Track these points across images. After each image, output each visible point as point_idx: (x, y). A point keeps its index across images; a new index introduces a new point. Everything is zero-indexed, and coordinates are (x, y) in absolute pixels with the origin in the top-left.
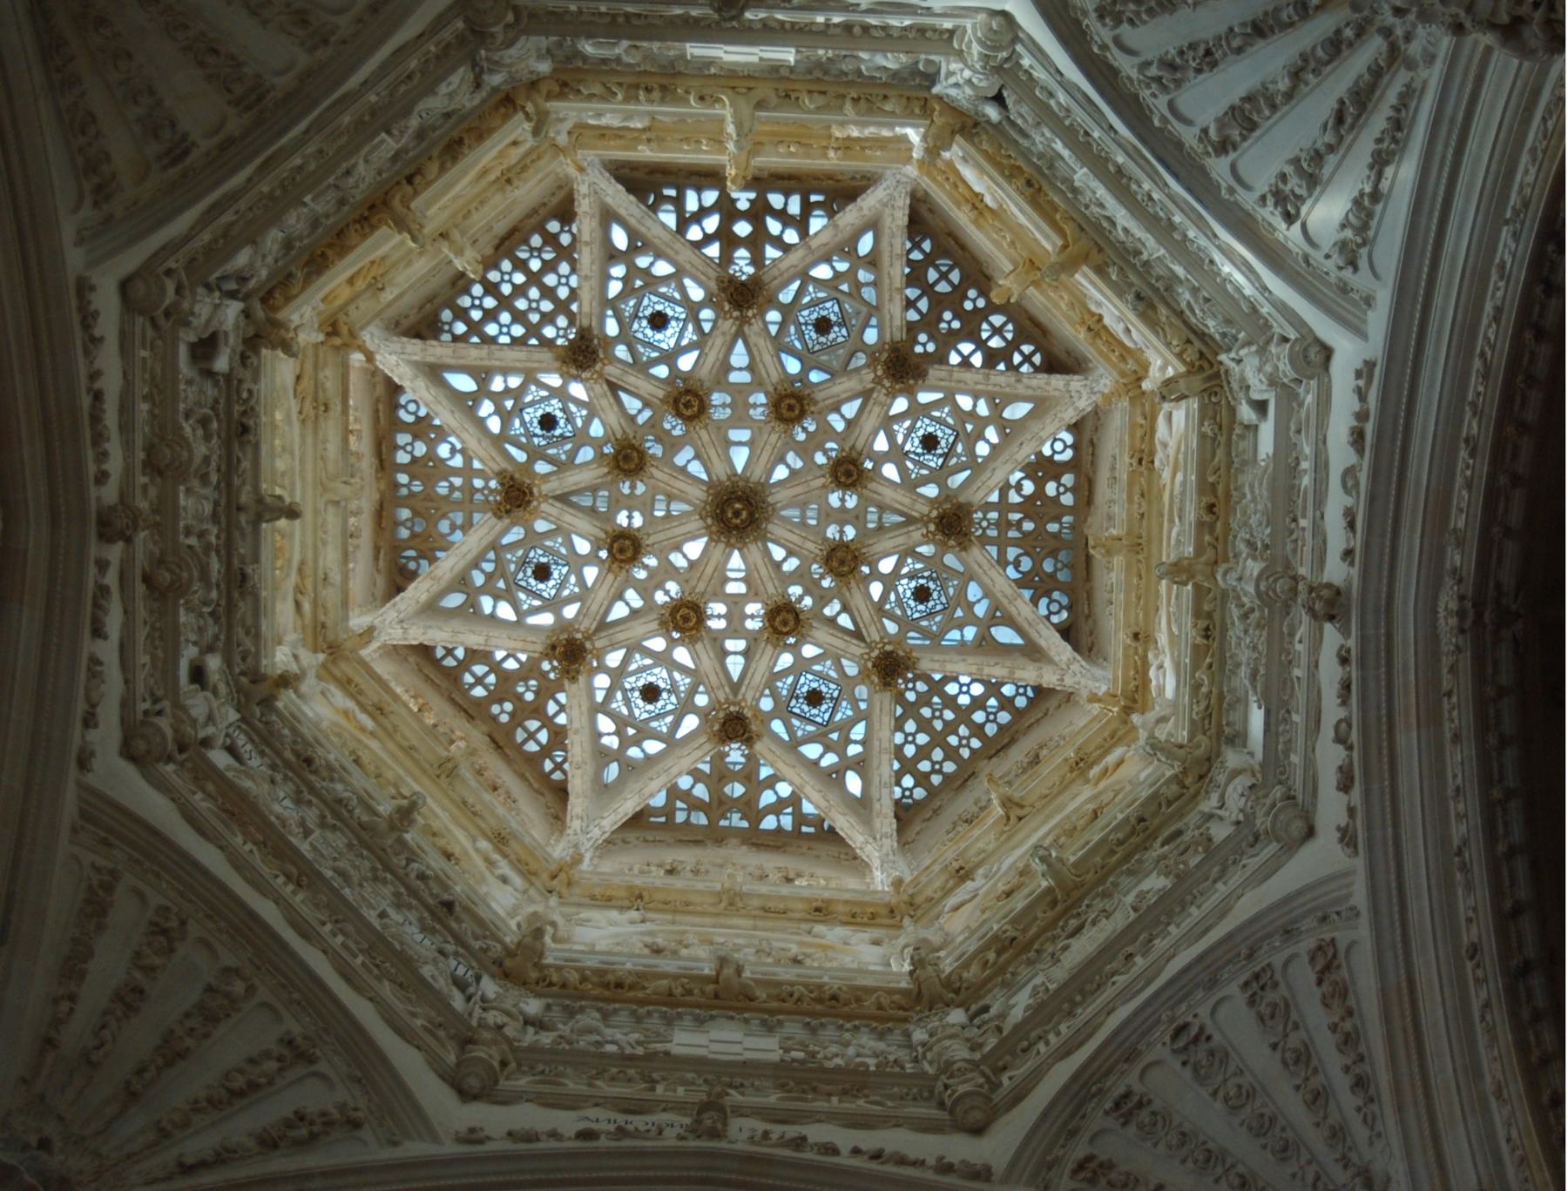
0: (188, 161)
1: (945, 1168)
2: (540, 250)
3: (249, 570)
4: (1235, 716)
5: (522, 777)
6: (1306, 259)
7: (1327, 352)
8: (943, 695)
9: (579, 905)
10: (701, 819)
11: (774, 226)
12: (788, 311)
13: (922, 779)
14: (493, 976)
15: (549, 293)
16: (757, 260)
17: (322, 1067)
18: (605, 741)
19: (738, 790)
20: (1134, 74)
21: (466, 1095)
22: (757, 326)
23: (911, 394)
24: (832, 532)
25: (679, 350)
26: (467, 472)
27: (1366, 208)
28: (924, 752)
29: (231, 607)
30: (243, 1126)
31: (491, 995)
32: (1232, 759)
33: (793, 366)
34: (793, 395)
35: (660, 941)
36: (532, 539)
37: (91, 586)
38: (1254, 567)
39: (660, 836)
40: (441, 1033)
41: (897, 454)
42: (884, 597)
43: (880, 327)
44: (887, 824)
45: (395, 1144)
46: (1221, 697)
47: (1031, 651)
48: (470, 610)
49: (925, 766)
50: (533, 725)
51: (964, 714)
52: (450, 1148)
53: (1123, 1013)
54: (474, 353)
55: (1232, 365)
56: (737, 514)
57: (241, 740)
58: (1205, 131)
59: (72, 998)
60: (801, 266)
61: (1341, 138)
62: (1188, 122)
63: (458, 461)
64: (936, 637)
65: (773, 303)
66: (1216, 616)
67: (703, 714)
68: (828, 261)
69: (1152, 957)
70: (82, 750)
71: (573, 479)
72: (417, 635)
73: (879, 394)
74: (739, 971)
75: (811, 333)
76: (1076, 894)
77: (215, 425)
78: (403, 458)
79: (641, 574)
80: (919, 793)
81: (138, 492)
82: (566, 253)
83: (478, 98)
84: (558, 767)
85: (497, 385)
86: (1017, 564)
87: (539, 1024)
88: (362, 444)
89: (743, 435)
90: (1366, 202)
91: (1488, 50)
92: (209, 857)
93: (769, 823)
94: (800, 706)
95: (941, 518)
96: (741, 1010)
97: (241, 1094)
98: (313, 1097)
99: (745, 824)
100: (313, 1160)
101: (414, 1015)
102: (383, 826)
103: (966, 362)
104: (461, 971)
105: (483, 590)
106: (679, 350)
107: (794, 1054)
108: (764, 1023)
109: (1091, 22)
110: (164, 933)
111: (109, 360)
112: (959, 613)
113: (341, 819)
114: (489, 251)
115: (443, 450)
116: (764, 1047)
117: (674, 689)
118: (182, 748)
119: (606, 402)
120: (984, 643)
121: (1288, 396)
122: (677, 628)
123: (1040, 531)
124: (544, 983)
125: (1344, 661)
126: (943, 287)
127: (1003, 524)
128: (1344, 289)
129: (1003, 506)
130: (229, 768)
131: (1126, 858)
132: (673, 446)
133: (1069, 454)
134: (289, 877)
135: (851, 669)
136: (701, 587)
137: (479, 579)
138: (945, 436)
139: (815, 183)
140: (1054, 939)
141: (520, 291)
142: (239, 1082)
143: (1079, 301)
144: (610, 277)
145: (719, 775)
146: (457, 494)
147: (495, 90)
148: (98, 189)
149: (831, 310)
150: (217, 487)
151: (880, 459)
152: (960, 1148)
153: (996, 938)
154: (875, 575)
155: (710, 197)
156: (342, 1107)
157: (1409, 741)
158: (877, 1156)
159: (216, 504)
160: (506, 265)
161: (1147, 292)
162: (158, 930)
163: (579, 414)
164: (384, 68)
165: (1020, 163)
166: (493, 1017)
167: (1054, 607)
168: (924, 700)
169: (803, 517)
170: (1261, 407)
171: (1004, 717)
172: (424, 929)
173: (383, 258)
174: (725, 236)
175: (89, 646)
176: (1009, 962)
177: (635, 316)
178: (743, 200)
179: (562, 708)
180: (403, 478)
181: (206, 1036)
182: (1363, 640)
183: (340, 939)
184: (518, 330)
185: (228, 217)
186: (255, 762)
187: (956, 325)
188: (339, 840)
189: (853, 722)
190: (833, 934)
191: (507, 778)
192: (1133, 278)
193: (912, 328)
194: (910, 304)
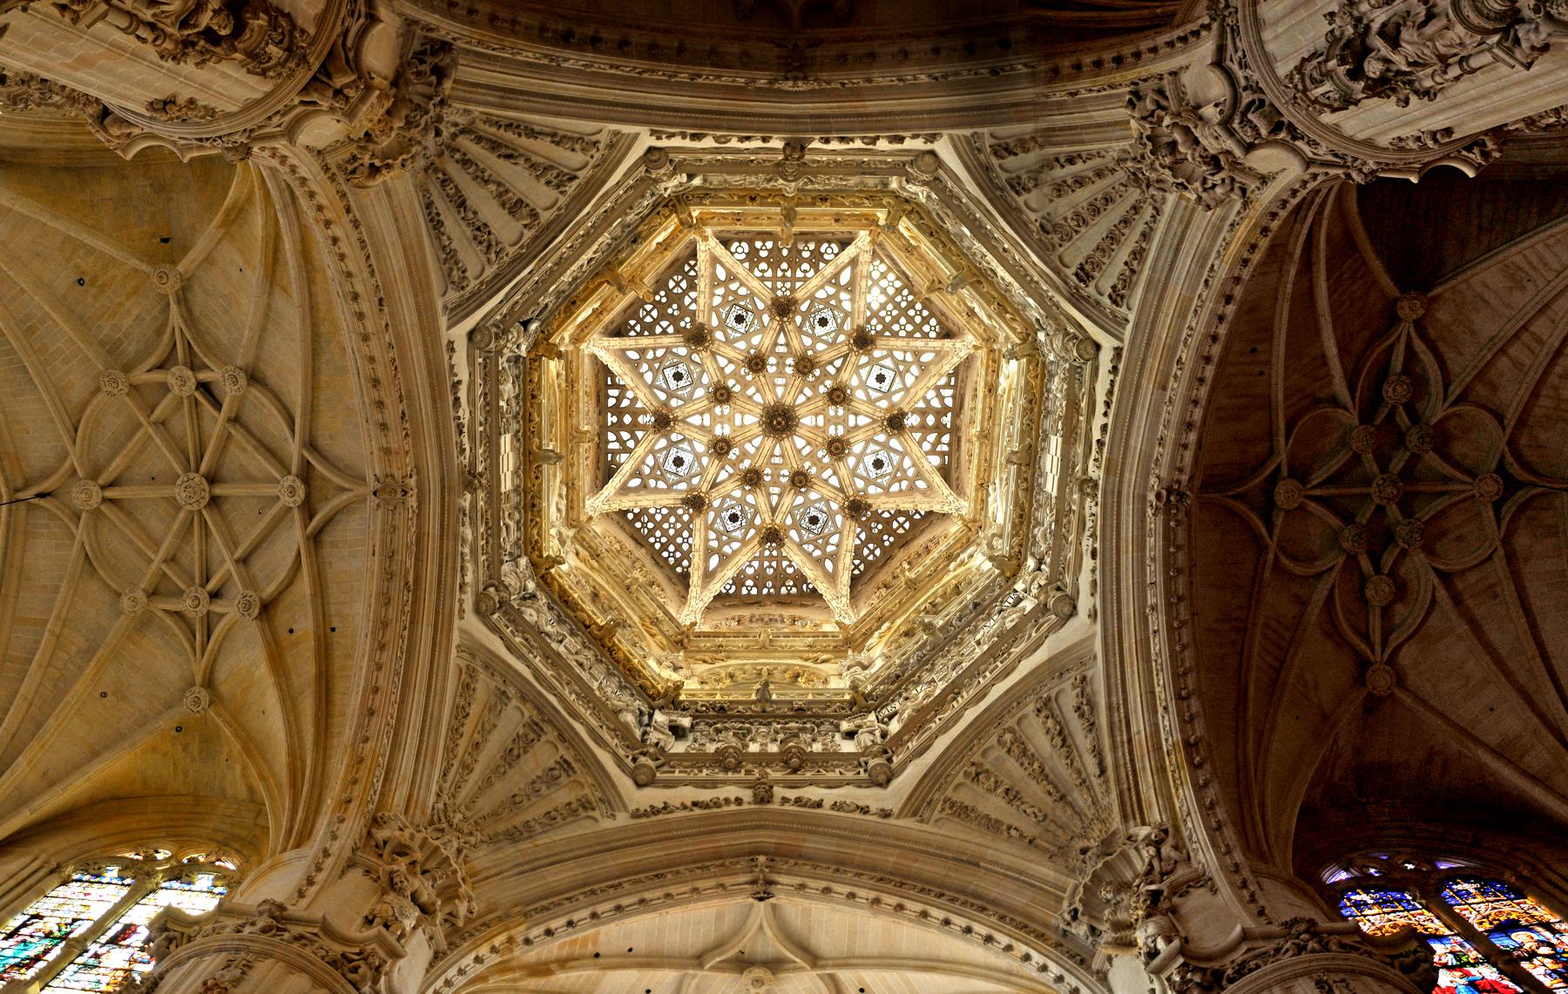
0: (570, 759)
5: (923, 531)
9: (986, 516)
10: (946, 438)
13: (925, 320)
14: (1015, 583)
15: (665, 518)
17: (1053, 693)
18: (904, 487)
20: (496, 267)
21: (1074, 611)
23: (711, 332)
25: (693, 451)
26: (761, 559)
28: (911, 320)
30: (1083, 741)
31: (1023, 586)
34: (715, 393)
36: (796, 526)
37: (794, 808)
40: (1041, 621)
44: (948, 343)
45: (1095, 657)
49: (918, 319)
50: (895, 525)
51: (891, 299)
52: (1098, 627)
54: (697, 559)
56: (779, 423)
57: (885, 712)
60: (647, 391)
61: (521, 155)
62: (522, 235)
64: (847, 314)
66: (814, 194)
67: (890, 436)
70: (880, 816)
71: (763, 506)
72: (846, 590)
77: (719, 725)
78: (754, 591)
80: (933, 322)
81: (749, 777)
82: (644, 511)
89: (738, 417)
90: (557, 139)
93: (949, 402)
94: (885, 386)
98: (1069, 699)
99: (949, 414)
101: (1030, 636)
104: (1010, 600)
105: (824, 551)
106: (693, 451)
107: (1060, 427)
112: (833, 302)
114: (643, 551)
115: (750, 571)
116: (1055, 442)
117: (877, 452)
118: (886, 752)
119: (722, 490)
122: (843, 452)
127: (784, 279)
129: (774, 279)
132: (744, 455)
134: (955, 699)
135: (864, 359)
136: (820, 440)
139: (601, 382)
141: (665, 533)
142: (1058, 740)
144: (656, 487)
145: (923, 428)
146: (774, 564)
148: (585, 808)
150: (751, 723)
154: (812, 347)
159: (761, 724)
160: (652, 540)
161: (631, 237)
163: (729, 502)
164: (520, 657)
165: (562, 308)
167: (829, 251)
168: (881, 320)
172: (989, 617)
173: (641, 618)
174: (634, 426)
175: (826, 810)
177: (676, 474)
180: (765, 591)
181: (1033, 755)
183: (987, 673)
184: (686, 534)
186: (897, 705)
187: (675, 306)
191: (922, 540)
192: (624, 244)
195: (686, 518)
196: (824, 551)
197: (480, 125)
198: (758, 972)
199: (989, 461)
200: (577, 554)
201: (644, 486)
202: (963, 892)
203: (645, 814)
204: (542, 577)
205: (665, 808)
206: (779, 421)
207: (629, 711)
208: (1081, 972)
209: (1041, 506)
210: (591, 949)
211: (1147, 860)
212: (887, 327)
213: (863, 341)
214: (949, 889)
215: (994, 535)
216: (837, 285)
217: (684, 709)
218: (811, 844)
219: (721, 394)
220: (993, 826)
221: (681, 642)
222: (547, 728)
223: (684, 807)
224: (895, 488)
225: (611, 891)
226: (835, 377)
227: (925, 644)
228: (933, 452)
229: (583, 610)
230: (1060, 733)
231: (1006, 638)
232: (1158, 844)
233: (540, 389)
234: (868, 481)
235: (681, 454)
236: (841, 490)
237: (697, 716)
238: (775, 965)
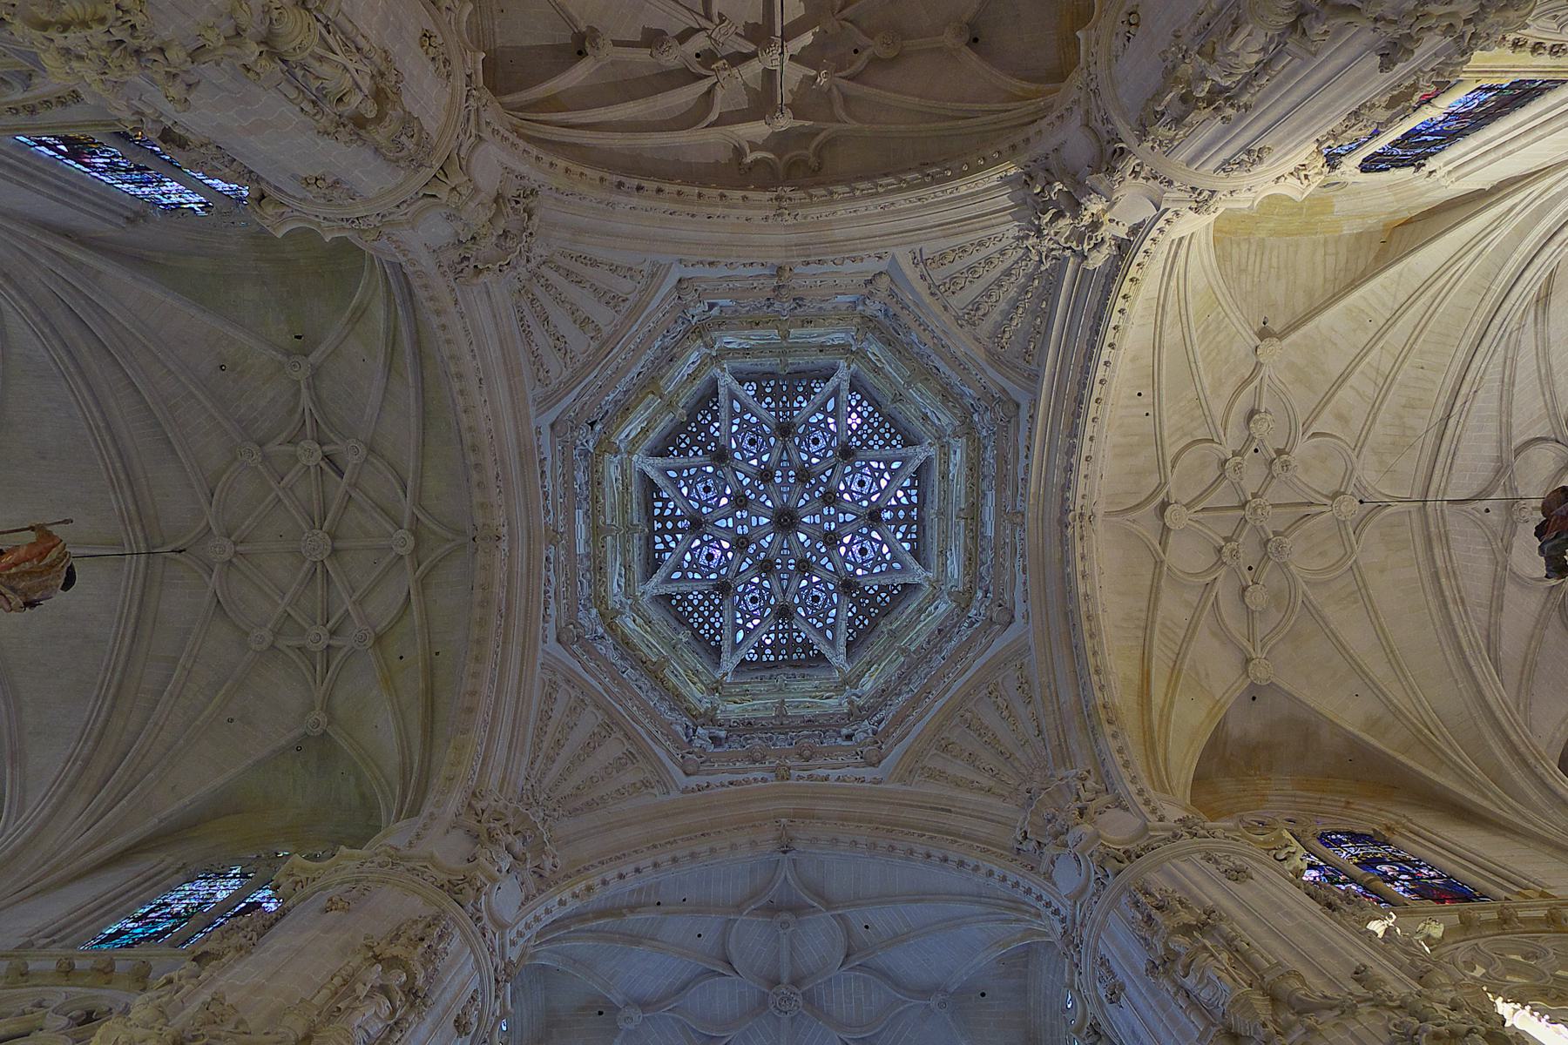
2: (684, 607)
3: (806, 719)
5: (900, 602)
8: (857, 429)
11: (668, 512)
12: (702, 504)
13: (893, 437)
15: (701, 602)
16: (681, 518)
17: (1000, 680)
19: (901, 514)
22: (708, 517)
24: (792, 480)
28: (882, 437)
33: (724, 501)
36: (802, 604)
39: (921, 544)
41: (758, 456)
42: (817, 457)
44: (910, 450)
47: (835, 393)
48: (832, 627)
49: (887, 436)
54: (727, 632)
55: (695, 319)
56: (786, 520)
58: (592, 338)
63: (772, 636)
68: (681, 488)
71: (776, 589)
72: (843, 649)
75: (710, 495)
79: (814, 558)
80: (899, 437)
82: (685, 595)
84: (896, 588)
85: (740, 621)
86: (800, 402)
89: (754, 519)
93: (914, 499)
95: (782, 436)
102: (908, 659)
104: (966, 625)
106: (721, 548)
108: (983, 498)
112: (822, 425)
113: (906, 677)
115: (768, 642)
116: (991, 495)
117: (862, 542)
119: (745, 578)
120: (834, 414)
124: (970, 592)
126: (688, 441)
131: (906, 350)
132: (760, 548)
137: (820, 625)
138: (749, 436)
139: (649, 496)
141: (701, 614)
143: (683, 384)
147: (605, 631)
149: (700, 486)
151: (760, 462)
155: (658, 539)
159: (780, 733)
162: (945, 749)
167: (818, 385)
168: (859, 438)
170: (711, 306)
172: (951, 639)
174: (673, 533)
175: (831, 782)
176: (953, 397)
178: (658, 525)
179: (871, 588)
180: (781, 657)
184: (717, 614)
185: (659, 737)
194: (696, 454)
198: (786, 916)
199: (945, 532)
200: (634, 621)
201: (684, 578)
203: (693, 791)
204: (608, 625)
205: (708, 786)
206: (785, 521)
209: (984, 549)
212: (864, 443)
213: (846, 453)
216: (824, 412)
219: (739, 501)
221: (717, 689)
224: (876, 570)
225: (668, 846)
228: (903, 540)
233: (603, 478)
234: (856, 566)
237: (730, 729)
238: (798, 909)
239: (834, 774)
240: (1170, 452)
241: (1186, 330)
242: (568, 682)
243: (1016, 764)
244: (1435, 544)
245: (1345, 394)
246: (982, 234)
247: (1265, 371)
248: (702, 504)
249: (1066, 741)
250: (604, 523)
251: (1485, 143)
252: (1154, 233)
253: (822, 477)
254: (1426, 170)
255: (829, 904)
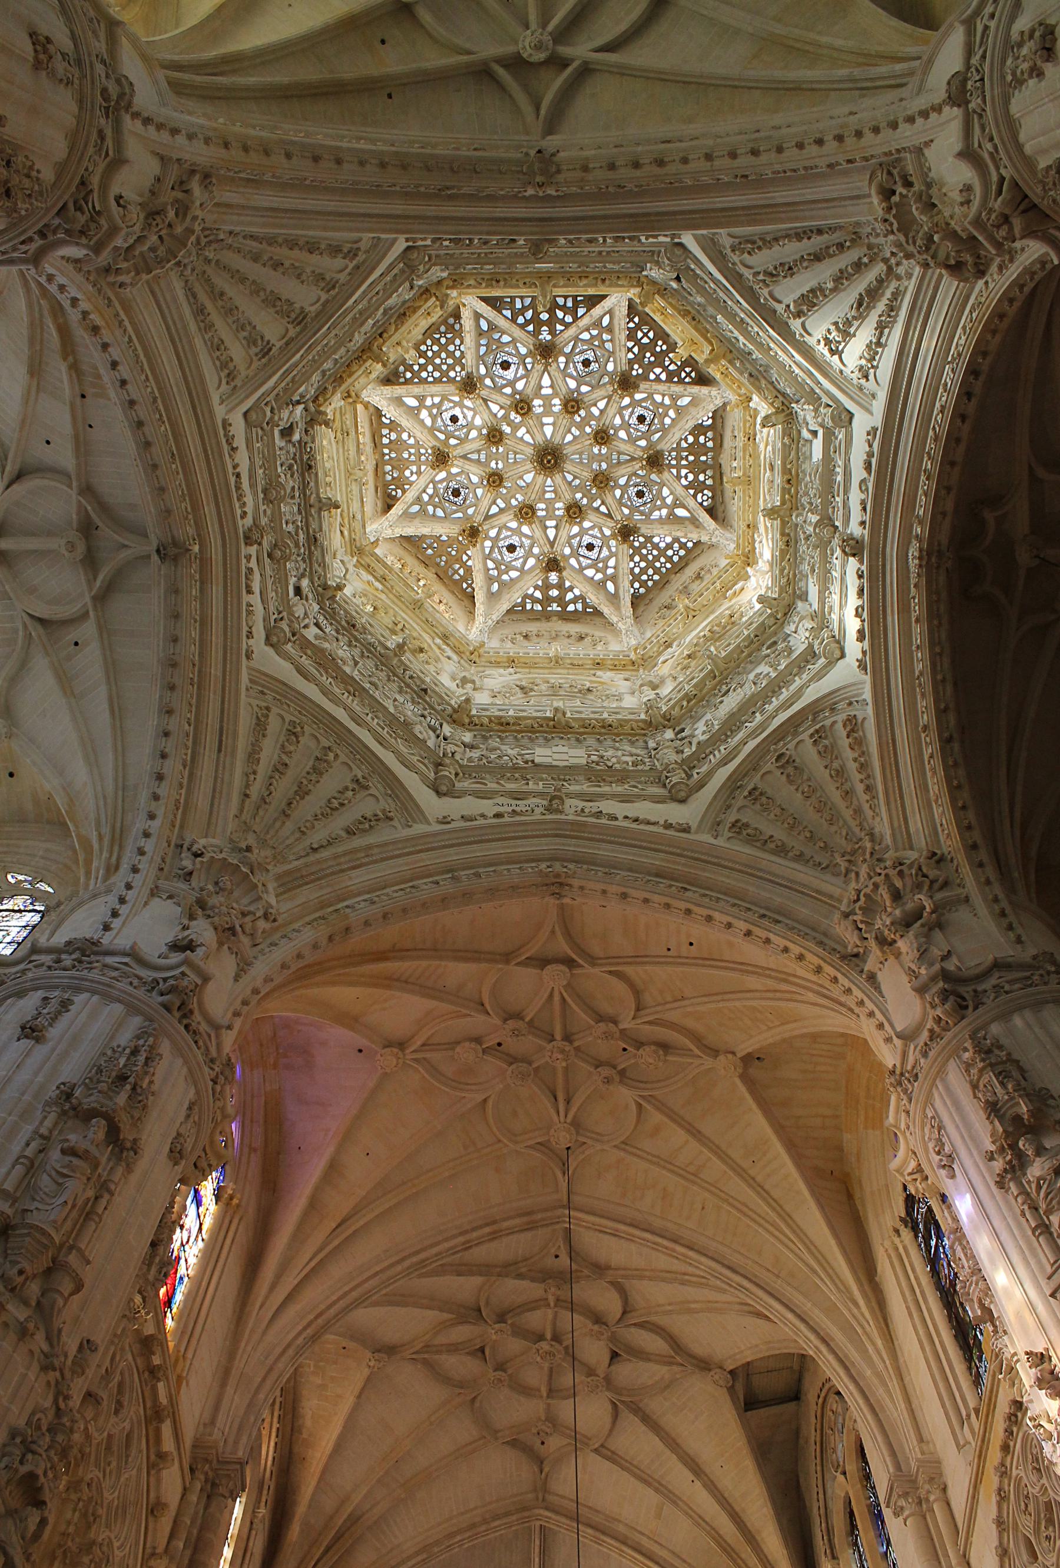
1: (668, 826)
4: (802, 584)
5: (453, 593)
6: (841, 372)
7: (851, 416)
11: (560, 314)
12: (569, 357)
13: (643, 584)
16: (552, 332)
17: (373, 791)
22: (554, 365)
24: (595, 466)
25: (517, 379)
27: (875, 347)
28: (643, 571)
29: (311, 553)
32: (800, 604)
33: (572, 384)
35: (524, 683)
38: (814, 518)
39: (519, 616)
41: (626, 425)
42: (622, 496)
43: (615, 362)
44: (627, 609)
46: (795, 575)
47: (694, 521)
51: (662, 552)
53: (752, 745)
54: (417, 390)
57: (321, 619)
58: (788, 306)
59: (255, 773)
65: (561, 353)
69: (766, 716)
72: (398, 532)
73: (616, 397)
74: (564, 714)
75: (580, 366)
76: (725, 673)
80: (642, 590)
83: (412, 293)
87: (472, 747)
88: (365, 439)
91: (941, 276)
92: (311, 691)
94: (583, 551)
95: (649, 458)
96: (566, 734)
97: (337, 809)
100: (371, 839)
102: (391, 654)
103: (658, 379)
105: (428, 503)
106: (517, 379)
108: (578, 740)
109: (728, 251)
110: (293, 733)
111: (243, 458)
115: (405, 436)
118: (294, 635)
121: (829, 435)
123: (697, 460)
124: (472, 725)
125: (860, 577)
126: (645, 340)
127: (679, 458)
128: (861, 388)
129: (678, 449)
130: (316, 637)
131: (750, 655)
132: (515, 428)
133: (710, 422)
137: (426, 498)
138: (649, 416)
140: (715, 695)
141: (437, 354)
145: (547, 586)
147: (420, 287)
148: (229, 375)
149: (590, 356)
152: (676, 813)
153: (686, 694)
156: (384, 811)
157: (893, 620)
158: (636, 820)
163: (470, 414)
166: (450, 748)
168: (643, 546)
169: (581, 458)
170: (815, 433)
171: (682, 553)
175: (246, 598)
182: (870, 568)
184: (437, 374)
188: (370, 663)
189: (609, 558)
190: (606, 676)
193: (631, 362)
194: (630, 350)
195: (452, 374)
196: (428, 503)
197: (894, 284)
201: (480, 333)
202: (195, 743)
204: (427, 290)
207: (308, 389)
208: (153, 872)
210: (89, 391)
211: (252, 908)
213: (626, 533)
214: (196, 729)
215: (473, 682)
217: (306, 431)
218: (216, 591)
219: (572, 404)
220: (253, 757)
221: (349, 396)
222: (298, 329)
223: (235, 467)
224: (490, 564)
226: (589, 505)
227: (387, 648)
229: (396, 330)
230: (342, 805)
231: (403, 728)
232: (266, 916)
235: (513, 367)
236: (487, 517)
239: (255, 599)
240: (629, 970)
241: (758, 994)
242: (357, 267)
243: (278, 824)
244: (525, 1219)
245: (679, 1136)
246: (880, 787)
247: (708, 1062)
248: (569, 357)
249: (307, 884)
250: (554, 286)
251: (922, 1293)
252: (870, 1005)
253: (599, 502)
254: (902, 1228)
255: (102, 598)
